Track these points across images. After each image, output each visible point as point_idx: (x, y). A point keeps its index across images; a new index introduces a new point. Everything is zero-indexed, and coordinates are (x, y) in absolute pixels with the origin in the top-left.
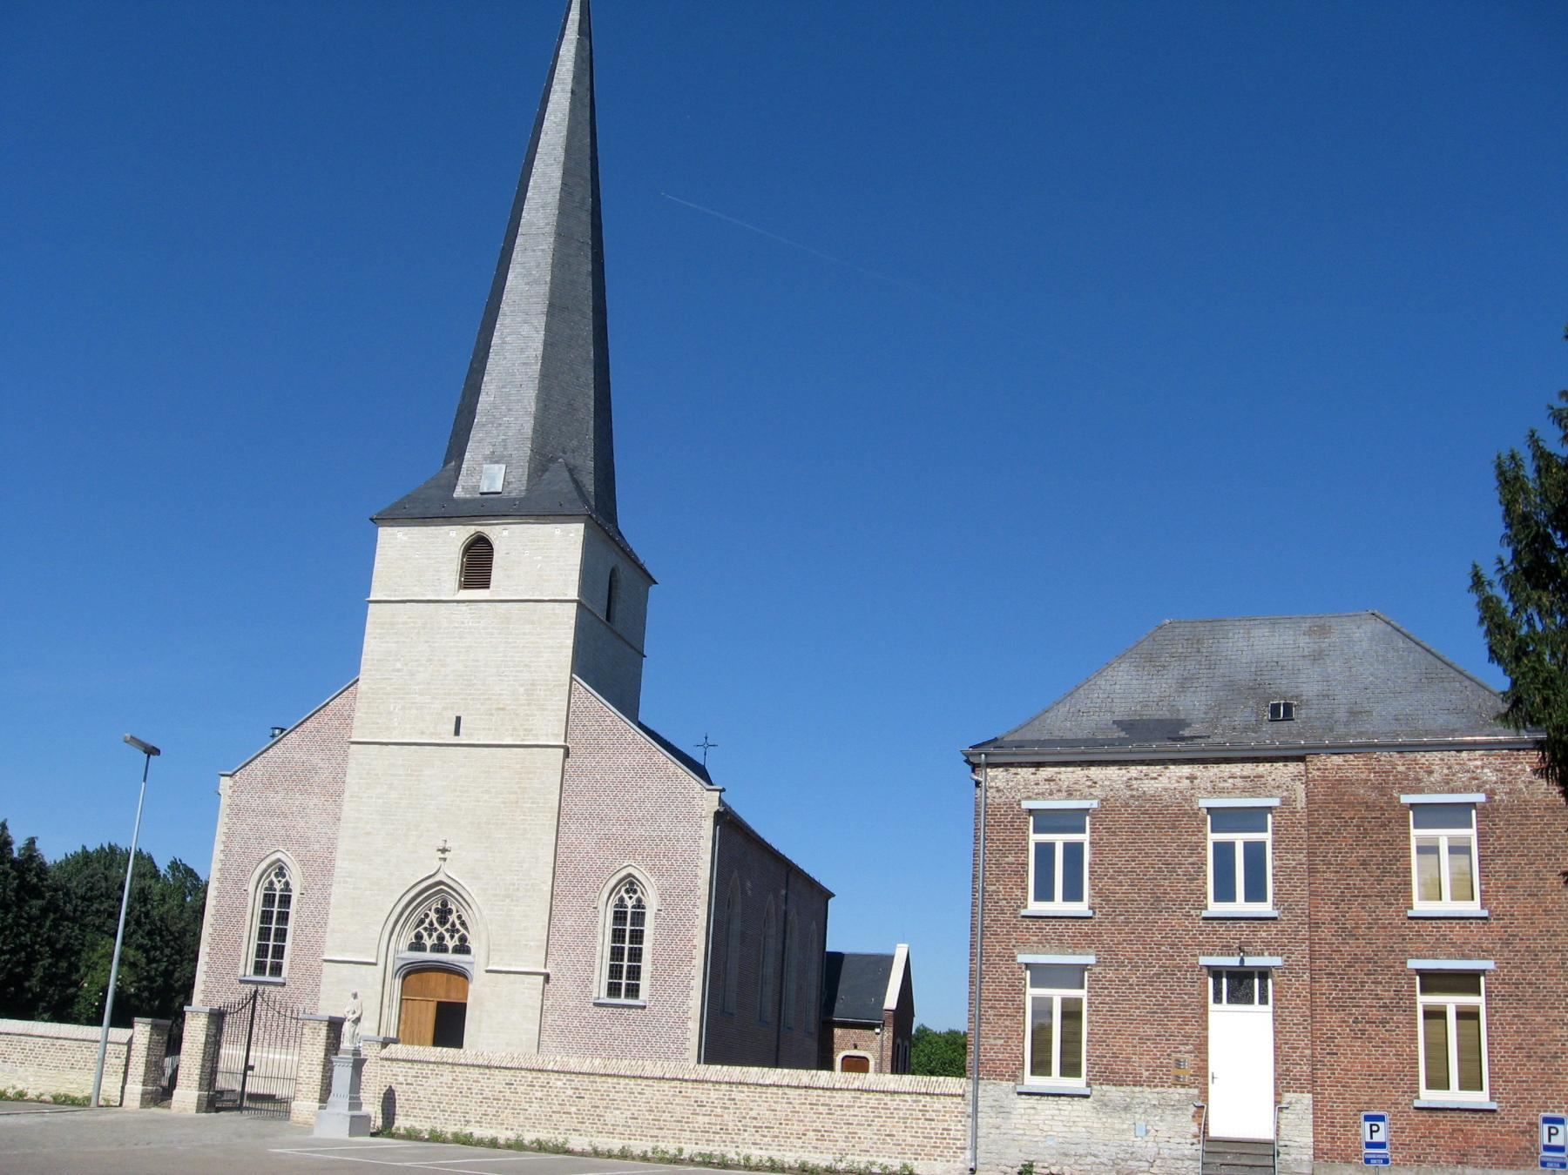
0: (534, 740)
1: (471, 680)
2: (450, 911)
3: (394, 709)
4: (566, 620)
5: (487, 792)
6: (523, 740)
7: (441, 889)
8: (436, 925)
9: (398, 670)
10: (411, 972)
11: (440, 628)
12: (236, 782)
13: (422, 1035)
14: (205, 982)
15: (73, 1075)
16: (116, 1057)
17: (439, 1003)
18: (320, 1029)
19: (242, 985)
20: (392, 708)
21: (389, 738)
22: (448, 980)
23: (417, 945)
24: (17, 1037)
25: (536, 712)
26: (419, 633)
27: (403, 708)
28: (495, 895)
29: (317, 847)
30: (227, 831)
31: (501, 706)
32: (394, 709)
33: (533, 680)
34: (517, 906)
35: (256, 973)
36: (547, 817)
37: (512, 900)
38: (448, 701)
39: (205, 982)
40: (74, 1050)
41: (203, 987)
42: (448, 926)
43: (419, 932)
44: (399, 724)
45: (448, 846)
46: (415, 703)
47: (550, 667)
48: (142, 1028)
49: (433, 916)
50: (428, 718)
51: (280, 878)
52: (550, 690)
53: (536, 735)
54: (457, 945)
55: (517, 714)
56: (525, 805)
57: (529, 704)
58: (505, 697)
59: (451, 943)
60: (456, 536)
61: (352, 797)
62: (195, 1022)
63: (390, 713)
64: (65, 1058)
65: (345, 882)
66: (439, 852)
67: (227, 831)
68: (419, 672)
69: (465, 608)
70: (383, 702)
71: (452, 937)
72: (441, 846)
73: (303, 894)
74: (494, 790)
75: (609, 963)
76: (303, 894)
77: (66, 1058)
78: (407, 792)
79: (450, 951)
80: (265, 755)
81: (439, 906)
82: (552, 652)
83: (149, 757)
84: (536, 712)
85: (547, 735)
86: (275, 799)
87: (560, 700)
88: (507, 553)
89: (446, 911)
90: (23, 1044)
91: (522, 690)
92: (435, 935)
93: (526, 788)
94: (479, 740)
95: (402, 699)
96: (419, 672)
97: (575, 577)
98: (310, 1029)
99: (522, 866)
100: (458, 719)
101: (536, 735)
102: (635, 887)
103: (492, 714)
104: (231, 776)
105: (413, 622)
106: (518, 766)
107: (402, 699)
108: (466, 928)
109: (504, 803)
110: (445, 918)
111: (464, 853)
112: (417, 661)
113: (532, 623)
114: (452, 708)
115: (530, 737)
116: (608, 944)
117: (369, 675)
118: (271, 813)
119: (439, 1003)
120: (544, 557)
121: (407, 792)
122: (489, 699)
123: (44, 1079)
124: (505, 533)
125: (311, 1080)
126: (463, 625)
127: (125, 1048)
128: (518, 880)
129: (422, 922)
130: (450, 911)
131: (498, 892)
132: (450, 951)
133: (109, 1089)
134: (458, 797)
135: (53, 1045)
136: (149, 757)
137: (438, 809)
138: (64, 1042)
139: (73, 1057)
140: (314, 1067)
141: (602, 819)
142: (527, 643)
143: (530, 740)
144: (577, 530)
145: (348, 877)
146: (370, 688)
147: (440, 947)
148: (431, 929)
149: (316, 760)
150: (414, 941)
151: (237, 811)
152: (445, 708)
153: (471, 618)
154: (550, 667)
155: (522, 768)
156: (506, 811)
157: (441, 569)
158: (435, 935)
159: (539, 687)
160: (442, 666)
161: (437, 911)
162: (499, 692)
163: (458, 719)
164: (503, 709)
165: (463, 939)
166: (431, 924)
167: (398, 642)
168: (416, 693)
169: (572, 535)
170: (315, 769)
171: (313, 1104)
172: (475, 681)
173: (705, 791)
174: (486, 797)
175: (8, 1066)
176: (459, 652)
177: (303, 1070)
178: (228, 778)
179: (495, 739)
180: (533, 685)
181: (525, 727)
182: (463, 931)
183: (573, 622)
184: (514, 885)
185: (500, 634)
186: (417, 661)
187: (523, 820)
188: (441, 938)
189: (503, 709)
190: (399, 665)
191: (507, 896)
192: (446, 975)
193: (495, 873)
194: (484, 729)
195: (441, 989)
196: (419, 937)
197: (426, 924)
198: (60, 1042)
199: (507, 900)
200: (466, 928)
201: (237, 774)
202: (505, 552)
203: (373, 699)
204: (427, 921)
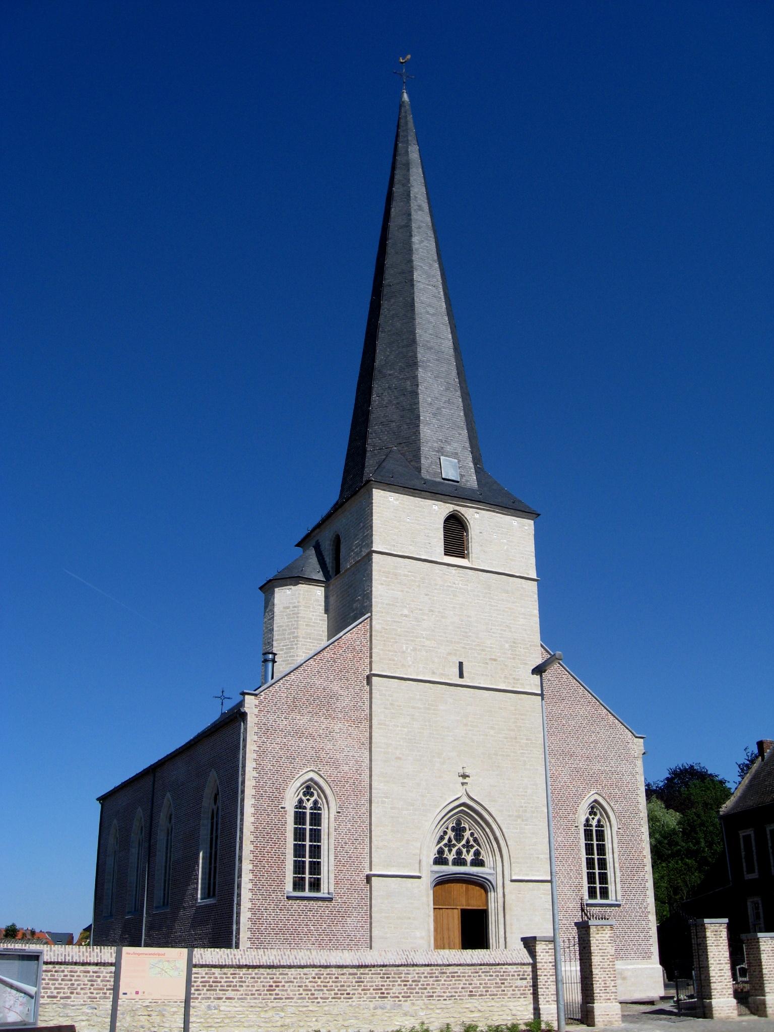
0: (521, 688)
1: (466, 633)
2: (464, 829)
3: (407, 649)
4: (531, 594)
5: (492, 728)
6: (513, 687)
7: (462, 810)
8: (454, 842)
9: (406, 616)
10: (442, 882)
11: (436, 585)
12: (261, 702)
13: (451, 939)
14: (251, 900)
15: (474, 1003)
16: (521, 979)
17: (462, 910)
18: (721, 931)
19: (290, 902)
20: (404, 648)
21: (406, 674)
22: (467, 889)
23: (440, 860)
24: (395, 969)
25: (520, 665)
26: (419, 586)
27: (414, 650)
28: (509, 816)
29: (346, 768)
30: (257, 749)
31: (493, 657)
32: (407, 649)
33: (515, 639)
34: (526, 825)
35: (295, 889)
36: (539, 751)
37: (523, 821)
38: (451, 648)
39: (251, 900)
40: (470, 976)
41: (249, 905)
42: (464, 842)
43: (441, 848)
44: (413, 663)
45: (468, 772)
46: (423, 646)
47: (525, 630)
48: (544, 947)
49: (451, 834)
50: (436, 660)
51: (308, 797)
52: (527, 648)
53: (522, 684)
54: (473, 859)
55: (506, 666)
56: (522, 741)
57: (514, 658)
58: (494, 650)
59: (469, 858)
60: (440, 510)
61: (379, 724)
62: (600, 935)
63: (404, 652)
64: (460, 986)
65: (383, 802)
66: (461, 778)
67: (257, 749)
68: (424, 620)
69: (454, 571)
70: (396, 642)
71: (468, 852)
72: (461, 772)
73: (339, 812)
74: (496, 727)
75: (321, 876)
76: (339, 812)
77: (462, 986)
78: (427, 723)
79: (469, 864)
80: (287, 678)
81: (454, 825)
82: (526, 618)
83: (541, 676)
84: (520, 665)
85: (530, 685)
86: (303, 721)
87: (536, 658)
88: (481, 533)
89: (460, 829)
90: (403, 975)
91: (507, 646)
92: (454, 850)
93: (521, 727)
94: (480, 683)
95: (412, 641)
96: (424, 620)
97: (533, 560)
98: (713, 932)
99: (526, 792)
100: (461, 664)
101: (522, 684)
102: (595, 810)
103: (487, 663)
104: (256, 695)
105: (413, 576)
106: (513, 708)
107: (412, 641)
108: (479, 845)
109: (506, 738)
110: (460, 836)
111: (481, 779)
112: (421, 610)
113: (507, 592)
114: (455, 654)
115: (518, 686)
116: (324, 860)
117: (381, 616)
118: (299, 734)
119: (462, 910)
120: (508, 541)
121: (427, 723)
122: (483, 650)
123: (438, 1011)
124: (477, 516)
125: (723, 978)
126: (454, 585)
127: (530, 969)
128: (525, 803)
129: (442, 838)
130: (464, 829)
131: (511, 813)
132: (469, 864)
133: (519, 1013)
134: (469, 730)
135: (443, 973)
136: (541, 676)
137: (455, 740)
138: (456, 969)
139: (471, 984)
140: (722, 966)
141: (571, 756)
142: (506, 608)
143: (518, 688)
144: (529, 525)
145: (386, 797)
146: (383, 628)
147: (459, 861)
148: (450, 845)
149: (336, 687)
150: (437, 856)
151: (265, 730)
152: (449, 654)
153: (461, 581)
154: (525, 630)
155: (515, 710)
156: (508, 745)
157: (430, 535)
158: (454, 850)
159: (519, 645)
160: (442, 617)
161: (453, 829)
162: (490, 645)
163: (461, 664)
164: (495, 660)
165: (477, 853)
166: (450, 840)
167: (402, 591)
168: (424, 638)
169: (526, 528)
170: (334, 696)
171: (730, 999)
172: (470, 634)
173: (634, 738)
174: (492, 732)
175: (388, 1002)
176: (454, 607)
177: (714, 970)
178: (253, 697)
179: (492, 684)
180: (514, 643)
181: (514, 676)
182: (477, 847)
183: (536, 596)
184: (522, 807)
185: (484, 597)
186: (421, 610)
187: (522, 753)
188: (459, 853)
189: (495, 660)
190: (406, 612)
191: (519, 817)
192: (464, 885)
193: (507, 796)
194: (483, 675)
195: (470, 899)
196: (441, 852)
197: (445, 841)
198: (451, 969)
199: (519, 820)
200: (479, 845)
201: (262, 694)
202: (479, 531)
203: (387, 638)
204: (447, 837)
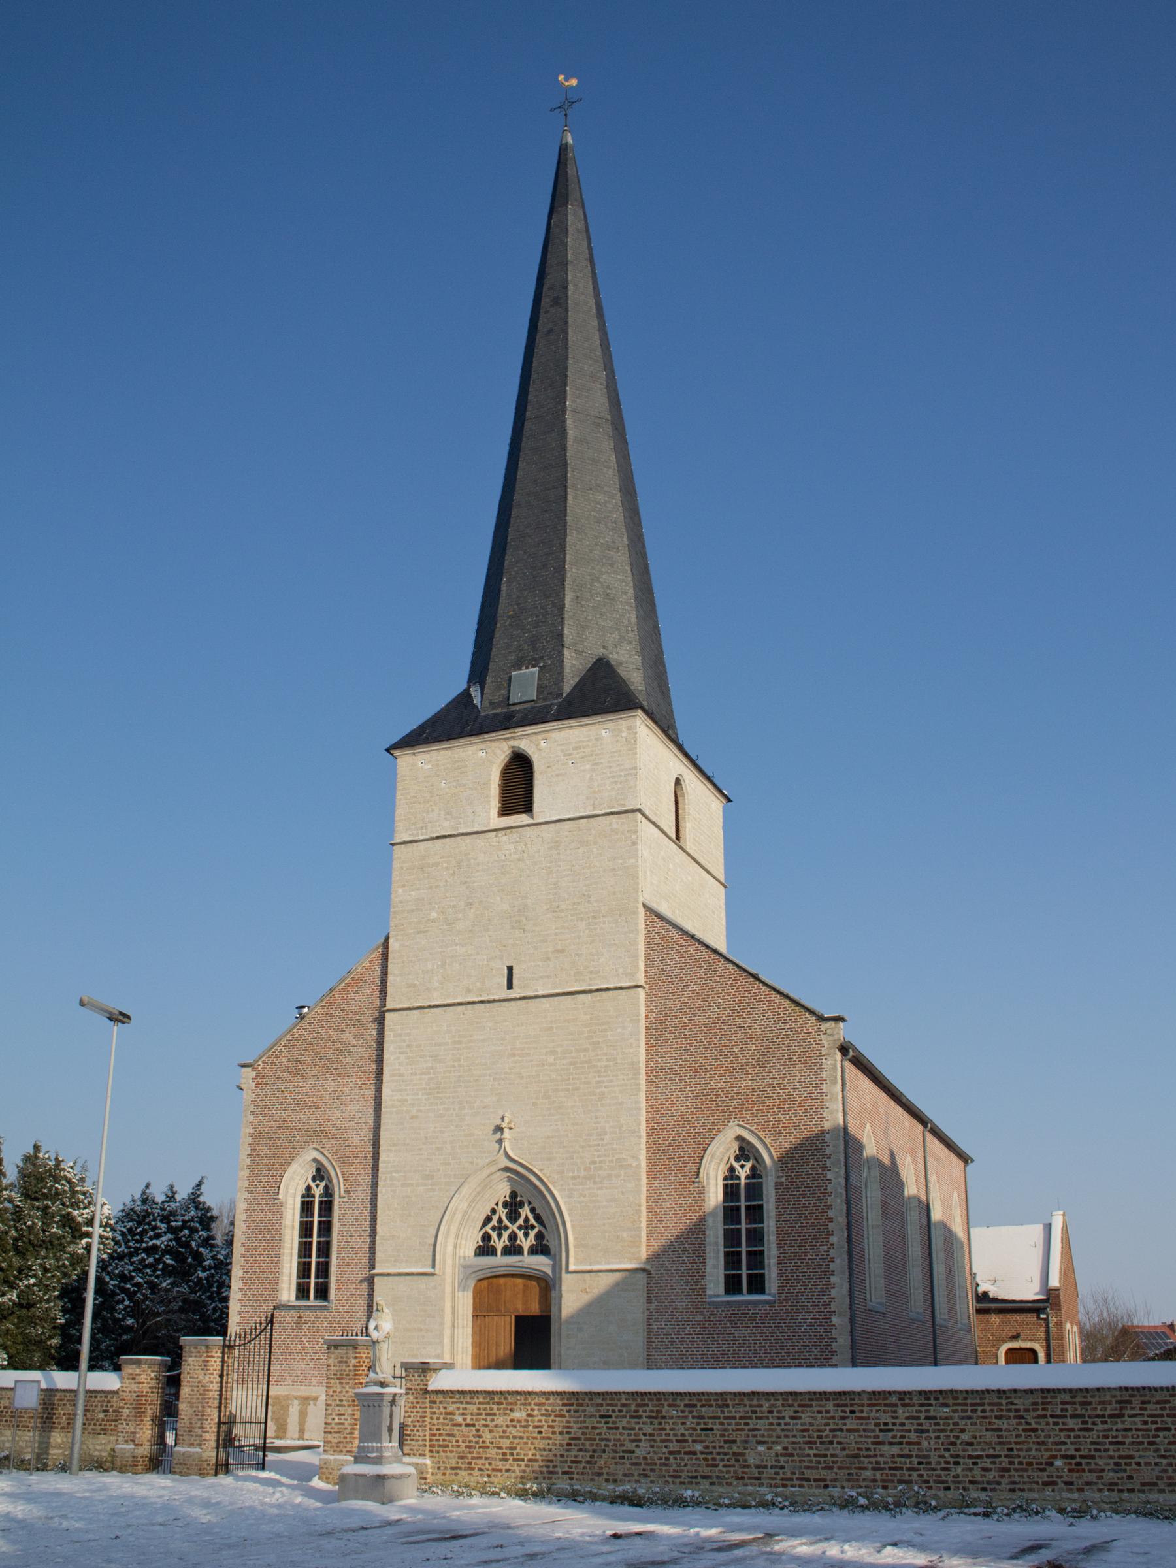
5: (553, 1052)
8: (506, 1222)
12: (259, 1073)
14: (240, 1312)
23: (485, 1249)
28: (574, 1178)
29: (356, 1140)
30: (252, 1131)
31: (559, 947)
34: (601, 1188)
35: (298, 1298)
39: (240, 1312)
42: (521, 1222)
49: (502, 1212)
51: (318, 1182)
54: (533, 1245)
59: (526, 1243)
67: (252, 1131)
71: (526, 1235)
92: (506, 1235)
93: (599, 1042)
100: (510, 969)
129: (488, 1219)
141: (696, 1071)
145: (396, 1172)
147: (513, 1249)
148: (500, 1228)
150: (481, 1243)
155: (591, 1019)
158: (506, 1235)
163: (510, 969)
164: (562, 951)
166: (500, 1221)
174: (551, 1059)
184: (595, 1162)
187: (599, 1082)
188: (513, 1237)
189: (562, 951)
196: (486, 1238)
197: (494, 1222)
204: (495, 1218)
